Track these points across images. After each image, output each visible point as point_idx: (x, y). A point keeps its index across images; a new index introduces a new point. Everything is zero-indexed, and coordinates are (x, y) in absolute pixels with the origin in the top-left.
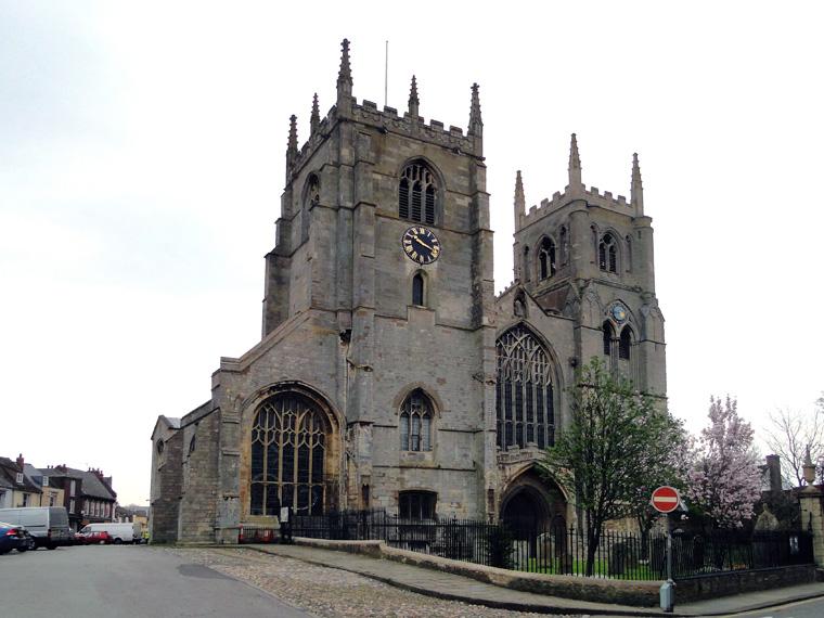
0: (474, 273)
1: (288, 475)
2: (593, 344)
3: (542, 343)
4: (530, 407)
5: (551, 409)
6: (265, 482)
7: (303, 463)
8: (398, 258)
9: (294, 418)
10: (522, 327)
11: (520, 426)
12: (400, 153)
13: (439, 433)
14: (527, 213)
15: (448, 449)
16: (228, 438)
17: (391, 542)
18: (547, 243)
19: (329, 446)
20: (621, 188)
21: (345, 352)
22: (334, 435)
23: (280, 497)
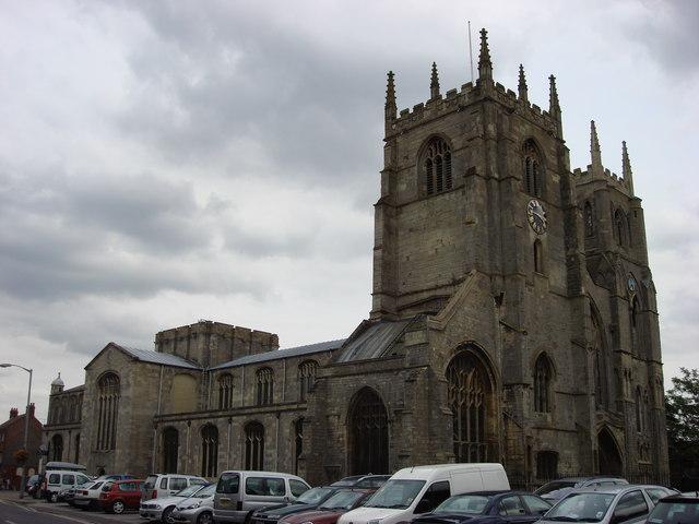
8: (526, 229)
12: (524, 130)
13: (556, 396)
19: (490, 402)
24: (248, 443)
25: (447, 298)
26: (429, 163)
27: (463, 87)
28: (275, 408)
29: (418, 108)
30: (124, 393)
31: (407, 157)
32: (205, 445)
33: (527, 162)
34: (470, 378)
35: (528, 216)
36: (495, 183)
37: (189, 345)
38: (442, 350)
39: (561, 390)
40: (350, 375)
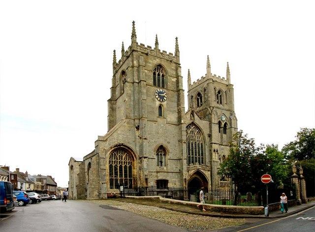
0: (178, 105)
1: (121, 175)
2: (215, 128)
3: (199, 129)
4: (196, 151)
5: (202, 151)
6: (114, 178)
7: (126, 172)
8: (154, 100)
9: (122, 156)
10: (193, 124)
11: (193, 157)
13: (169, 161)
14: (192, 84)
15: (172, 166)
16: (102, 163)
17: (163, 196)
18: (199, 94)
20: (223, 75)
21: (138, 133)
23: (119, 183)
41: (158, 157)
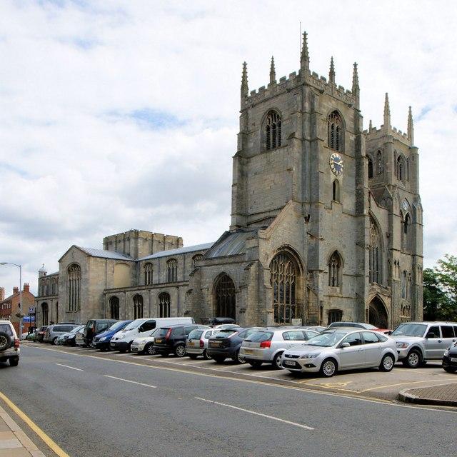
7: (288, 294)
8: (329, 173)
12: (326, 106)
21: (307, 227)
22: (301, 277)
24: (161, 305)
25: (274, 217)
26: (268, 129)
27: (291, 75)
28: (176, 284)
29: (262, 89)
30: (84, 276)
31: (254, 124)
32: (135, 306)
33: (333, 127)
34: (286, 267)
35: (330, 164)
36: (307, 143)
37: (124, 245)
38: (267, 250)
39: (347, 273)
40: (214, 265)
41: (330, 270)
